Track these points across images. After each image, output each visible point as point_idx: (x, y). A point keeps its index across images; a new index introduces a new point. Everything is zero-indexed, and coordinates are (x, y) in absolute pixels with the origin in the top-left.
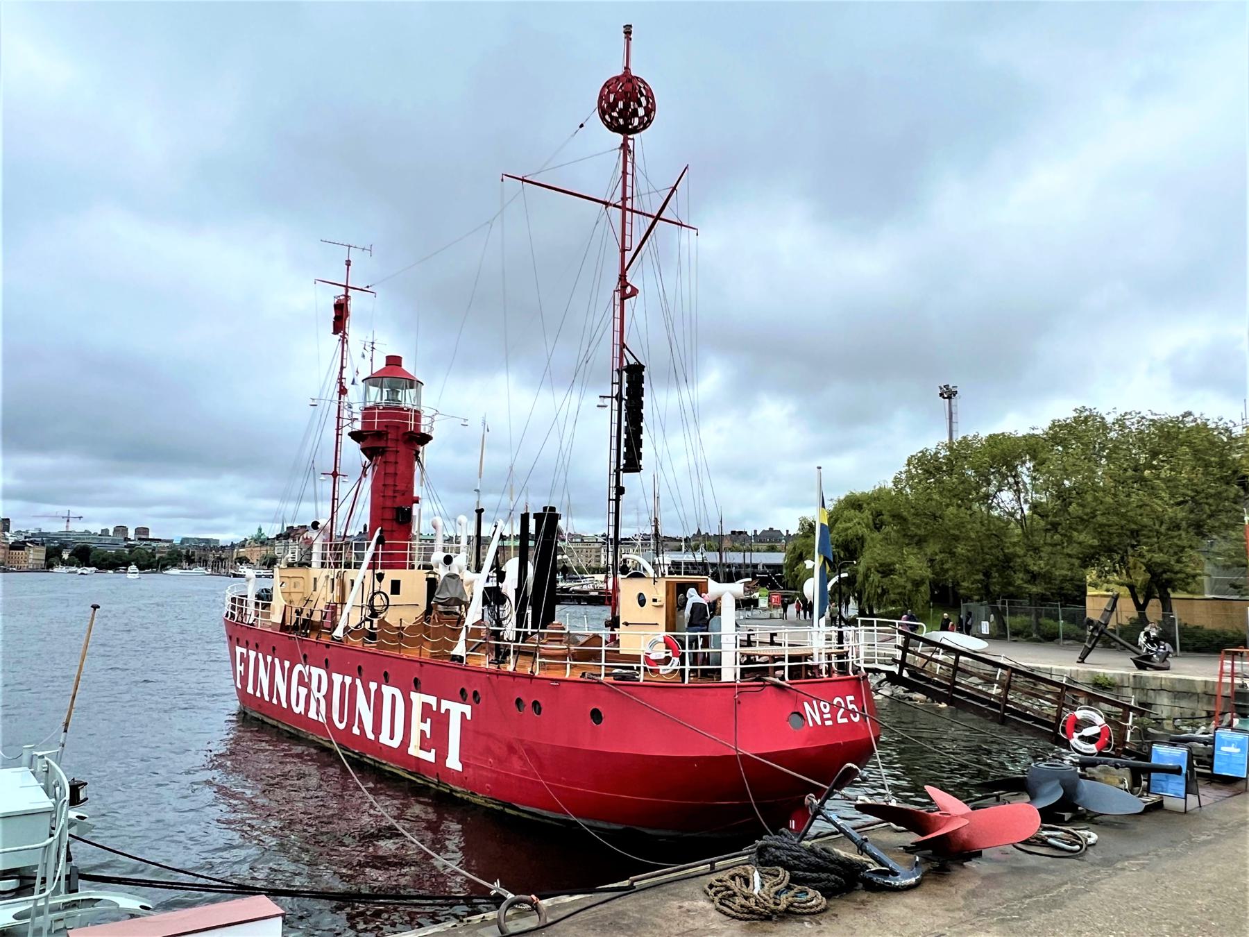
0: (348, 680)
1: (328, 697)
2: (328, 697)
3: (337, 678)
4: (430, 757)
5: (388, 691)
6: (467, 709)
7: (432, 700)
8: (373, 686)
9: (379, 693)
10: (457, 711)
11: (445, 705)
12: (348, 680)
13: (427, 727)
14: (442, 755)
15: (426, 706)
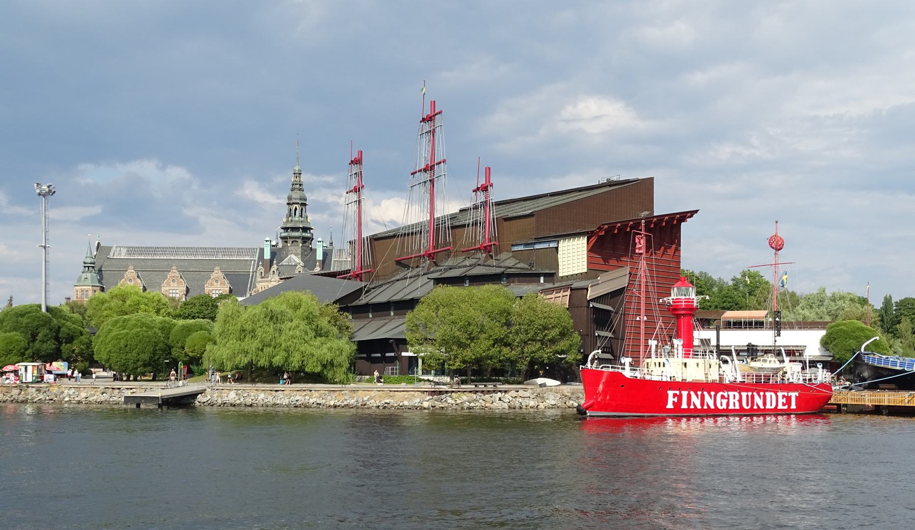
0: (750, 394)
1: (740, 401)
2: (740, 401)
3: (744, 394)
4: (786, 407)
5: (768, 394)
6: (797, 394)
7: (786, 394)
8: (762, 394)
9: (765, 396)
10: (794, 395)
11: (790, 394)
12: (750, 394)
13: (784, 401)
14: (790, 405)
15: (784, 396)
